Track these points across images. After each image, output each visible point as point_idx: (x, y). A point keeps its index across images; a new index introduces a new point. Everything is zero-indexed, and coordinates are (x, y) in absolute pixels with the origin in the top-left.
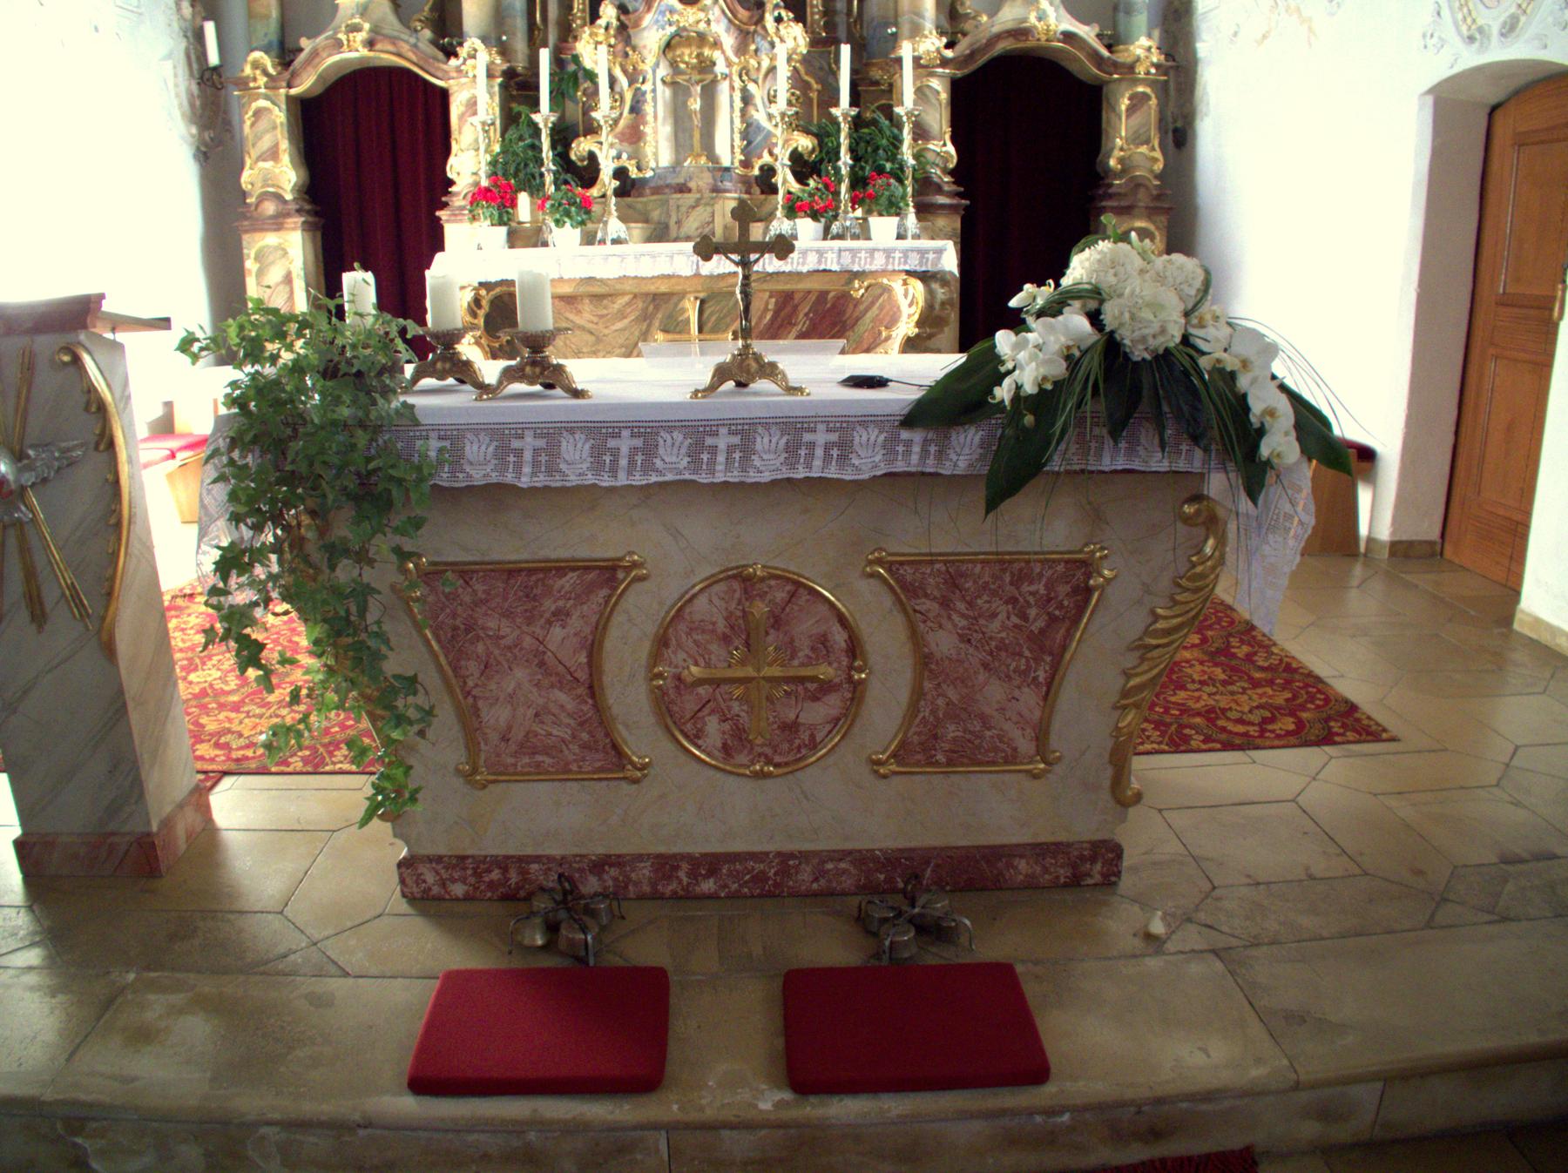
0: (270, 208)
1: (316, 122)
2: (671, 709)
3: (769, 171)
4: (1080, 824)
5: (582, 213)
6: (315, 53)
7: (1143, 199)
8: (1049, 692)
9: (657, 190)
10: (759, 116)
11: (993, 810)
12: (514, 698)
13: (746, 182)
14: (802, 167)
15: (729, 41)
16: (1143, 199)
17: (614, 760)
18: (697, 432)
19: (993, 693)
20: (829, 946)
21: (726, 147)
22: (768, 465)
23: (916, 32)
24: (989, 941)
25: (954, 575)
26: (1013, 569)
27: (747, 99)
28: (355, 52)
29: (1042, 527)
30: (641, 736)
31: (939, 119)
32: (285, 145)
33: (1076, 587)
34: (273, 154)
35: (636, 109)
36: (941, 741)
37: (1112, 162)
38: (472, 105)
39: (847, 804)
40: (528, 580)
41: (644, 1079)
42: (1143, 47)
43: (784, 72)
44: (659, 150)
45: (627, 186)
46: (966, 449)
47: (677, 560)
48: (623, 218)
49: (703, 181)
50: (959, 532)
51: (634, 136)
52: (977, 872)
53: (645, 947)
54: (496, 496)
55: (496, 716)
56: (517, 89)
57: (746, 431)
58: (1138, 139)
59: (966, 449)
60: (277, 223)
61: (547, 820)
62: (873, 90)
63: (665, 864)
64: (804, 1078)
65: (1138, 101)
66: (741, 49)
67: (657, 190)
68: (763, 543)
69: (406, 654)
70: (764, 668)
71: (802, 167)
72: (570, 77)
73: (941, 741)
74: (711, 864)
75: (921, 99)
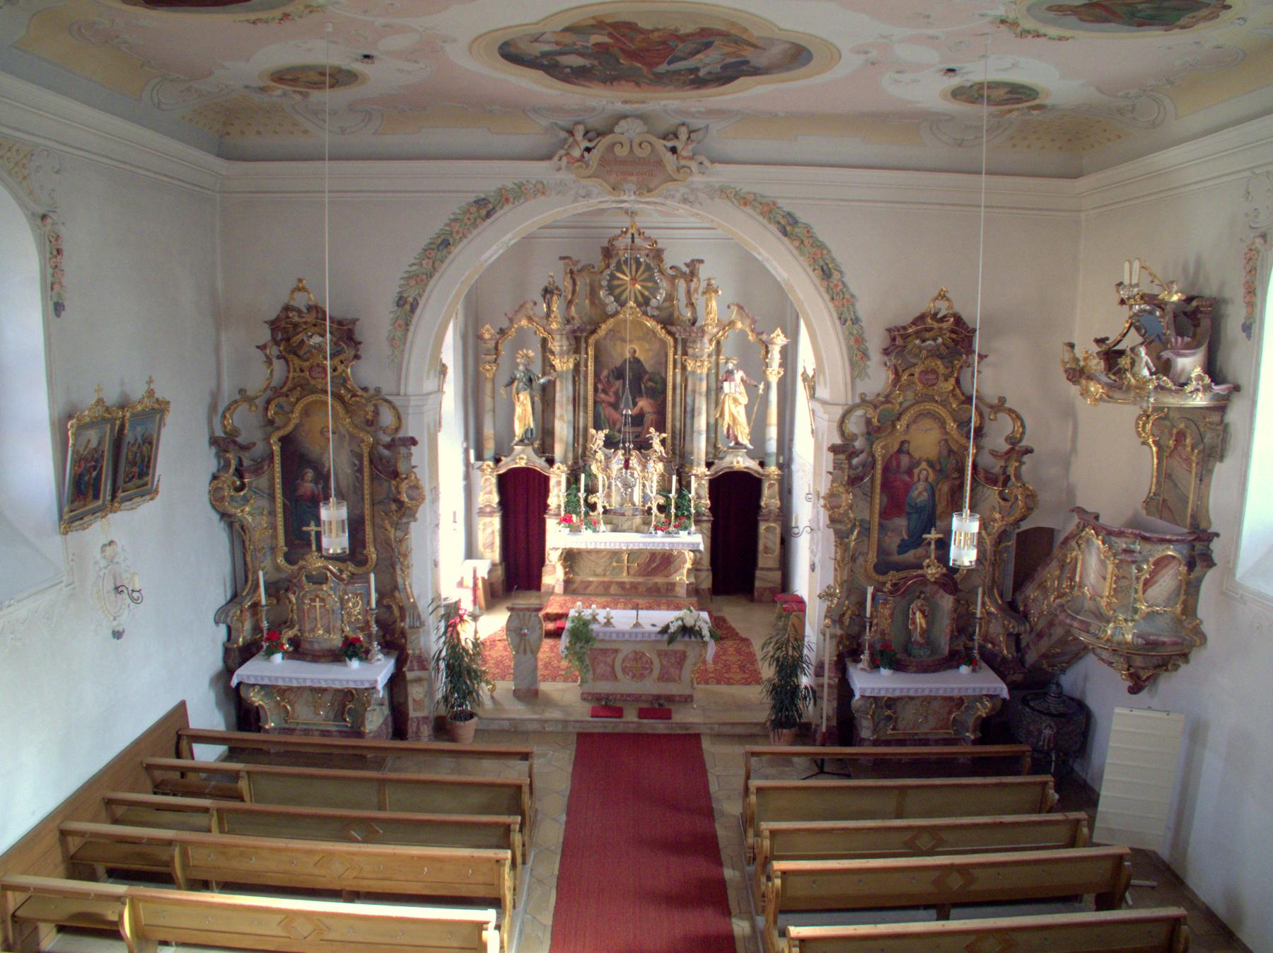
0: (488, 510)
1: (505, 483)
2: (624, 670)
3: (650, 509)
4: (687, 692)
5: (593, 525)
6: (507, 464)
7: (773, 516)
8: (681, 670)
9: (615, 513)
10: (648, 491)
11: (672, 689)
12: (602, 668)
13: (643, 511)
14: (661, 508)
15: (639, 469)
16: (773, 516)
17: (615, 678)
18: (630, 634)
19: (672, 670)
20: (645, 705)
21: (637, 498)
22: (639, 638)
23: (699, 465)
24: (667, 706)
25: (666, 653)
26: (675, 652)
27: (644, 485)
28: (522, 464)
29: (678, 646)
30: (620, 674)
31: (705, 492)
32: (495, 489)
33: (683, 656)
34: (490, 492)
35: (609, 487)
36: (664, 677)
37: (762, 504)
38: (559, 483)
39: (650, 687)
40: (604, 651)
41: (621, 716)
42: (773, 469)
43: (655, 478)
44: (615, 501)
45: (606, 512)
46: (666, 637)
47: (626, 650)
48: (606, 523)
49: (629, 513)
50: (664, 647)
51: (608, 496)
52: (670, 698)
53: (619, 704)
54: (602, 641)
55: (598, 671)
56: (573, 480)
57: (636, 634)
58: (771, 497)
59: (666, 637)
60: (491, 514)
61: (604, 687)
62: (684, 485)
63: (622, 695)
64: (640, 717)
65: (771, 486)
66: (643, 471)
67: (615, 513)
68: (638, 648)
69: (587, 662)
70: (638, 665)
71: (661, 508)
72: (591, 476)
73: (664, 677)
74: (629, 695)
75: (700, 476)
